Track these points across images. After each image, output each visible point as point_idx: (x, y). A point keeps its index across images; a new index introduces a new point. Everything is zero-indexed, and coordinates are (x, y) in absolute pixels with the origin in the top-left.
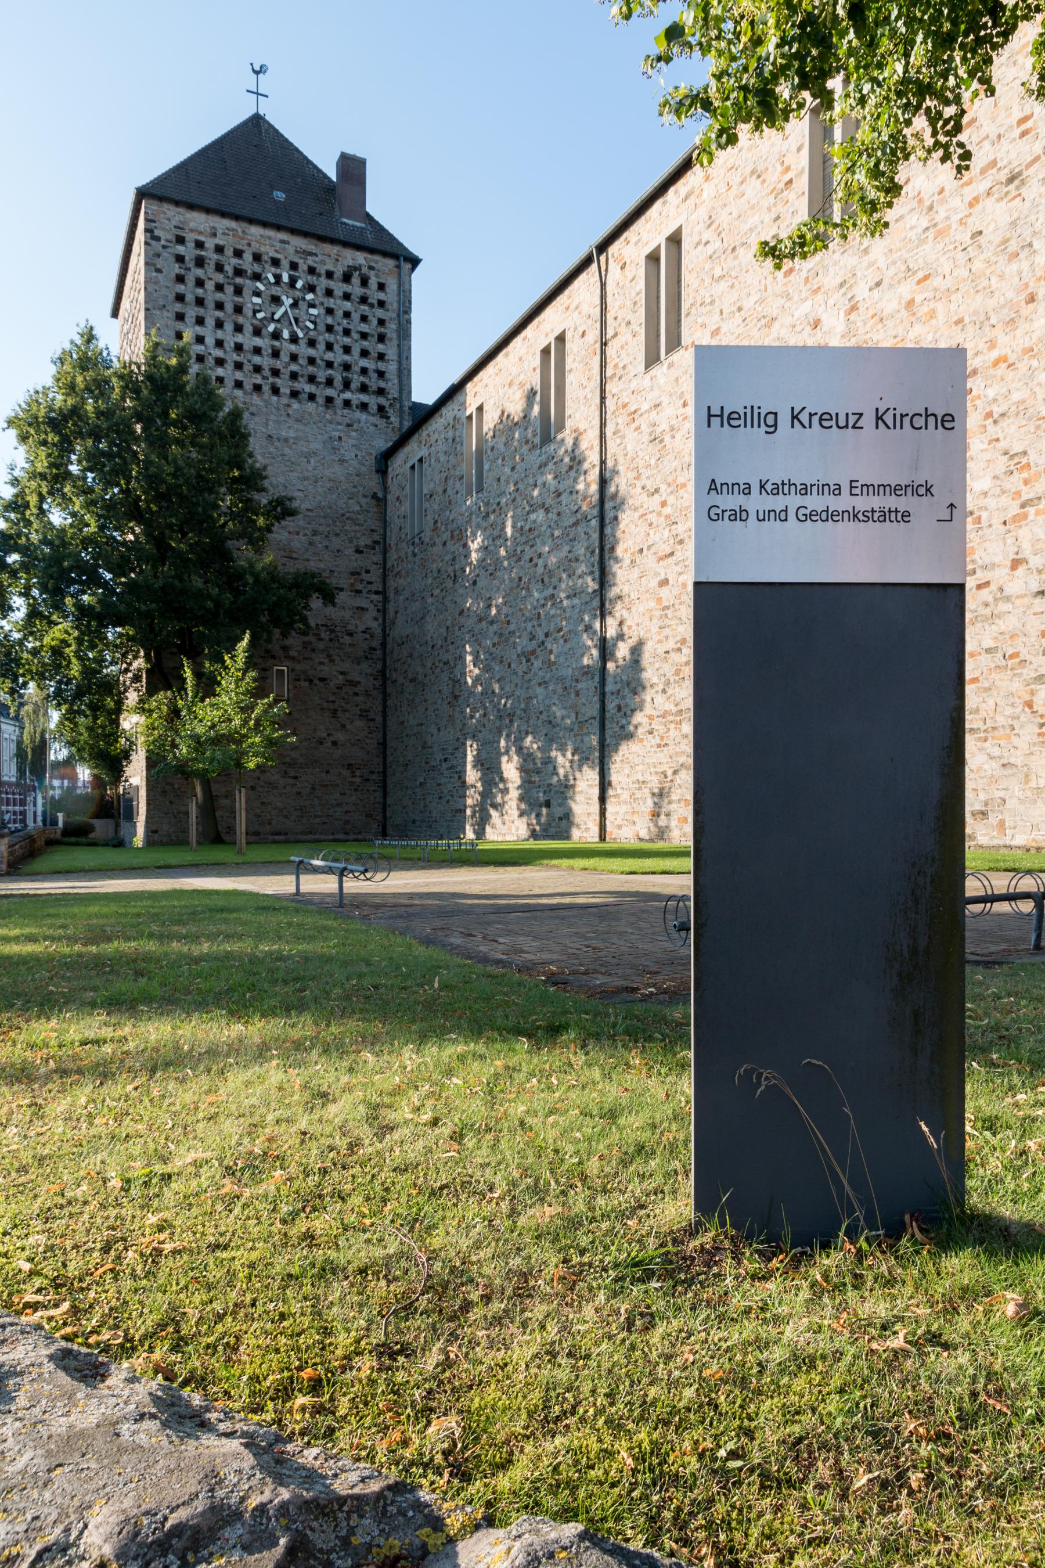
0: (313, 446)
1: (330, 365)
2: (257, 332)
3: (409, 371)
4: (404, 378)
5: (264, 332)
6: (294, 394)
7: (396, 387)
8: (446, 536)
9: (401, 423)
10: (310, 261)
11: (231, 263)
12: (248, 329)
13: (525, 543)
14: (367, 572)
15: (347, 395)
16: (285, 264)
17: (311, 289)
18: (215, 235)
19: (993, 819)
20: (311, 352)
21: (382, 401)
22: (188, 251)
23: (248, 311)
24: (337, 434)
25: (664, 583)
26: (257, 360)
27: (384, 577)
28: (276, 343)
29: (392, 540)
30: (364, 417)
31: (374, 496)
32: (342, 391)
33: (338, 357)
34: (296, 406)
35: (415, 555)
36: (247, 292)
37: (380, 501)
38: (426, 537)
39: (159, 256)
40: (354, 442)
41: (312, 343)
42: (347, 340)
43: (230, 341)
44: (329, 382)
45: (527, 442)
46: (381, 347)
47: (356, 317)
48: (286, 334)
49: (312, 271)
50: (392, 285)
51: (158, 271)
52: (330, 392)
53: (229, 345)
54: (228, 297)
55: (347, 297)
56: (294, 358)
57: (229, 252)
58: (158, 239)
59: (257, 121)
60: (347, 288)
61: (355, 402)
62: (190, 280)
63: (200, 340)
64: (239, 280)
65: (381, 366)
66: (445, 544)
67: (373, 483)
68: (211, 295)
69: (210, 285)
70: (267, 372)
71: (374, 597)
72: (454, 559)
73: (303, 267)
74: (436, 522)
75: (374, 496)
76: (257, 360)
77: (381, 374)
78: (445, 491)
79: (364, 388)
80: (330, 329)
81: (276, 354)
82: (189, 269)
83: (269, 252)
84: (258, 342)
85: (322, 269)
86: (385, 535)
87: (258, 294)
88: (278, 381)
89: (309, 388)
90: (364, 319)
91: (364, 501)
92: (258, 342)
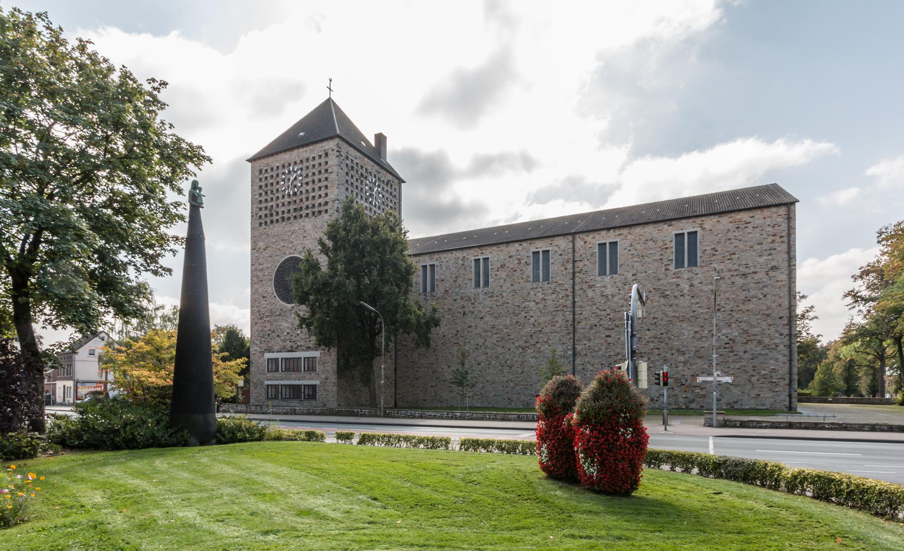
25: (609, 336)
54: (358, 184)
59: (329, 102)
68: (355, 184)
87: (366, 185)
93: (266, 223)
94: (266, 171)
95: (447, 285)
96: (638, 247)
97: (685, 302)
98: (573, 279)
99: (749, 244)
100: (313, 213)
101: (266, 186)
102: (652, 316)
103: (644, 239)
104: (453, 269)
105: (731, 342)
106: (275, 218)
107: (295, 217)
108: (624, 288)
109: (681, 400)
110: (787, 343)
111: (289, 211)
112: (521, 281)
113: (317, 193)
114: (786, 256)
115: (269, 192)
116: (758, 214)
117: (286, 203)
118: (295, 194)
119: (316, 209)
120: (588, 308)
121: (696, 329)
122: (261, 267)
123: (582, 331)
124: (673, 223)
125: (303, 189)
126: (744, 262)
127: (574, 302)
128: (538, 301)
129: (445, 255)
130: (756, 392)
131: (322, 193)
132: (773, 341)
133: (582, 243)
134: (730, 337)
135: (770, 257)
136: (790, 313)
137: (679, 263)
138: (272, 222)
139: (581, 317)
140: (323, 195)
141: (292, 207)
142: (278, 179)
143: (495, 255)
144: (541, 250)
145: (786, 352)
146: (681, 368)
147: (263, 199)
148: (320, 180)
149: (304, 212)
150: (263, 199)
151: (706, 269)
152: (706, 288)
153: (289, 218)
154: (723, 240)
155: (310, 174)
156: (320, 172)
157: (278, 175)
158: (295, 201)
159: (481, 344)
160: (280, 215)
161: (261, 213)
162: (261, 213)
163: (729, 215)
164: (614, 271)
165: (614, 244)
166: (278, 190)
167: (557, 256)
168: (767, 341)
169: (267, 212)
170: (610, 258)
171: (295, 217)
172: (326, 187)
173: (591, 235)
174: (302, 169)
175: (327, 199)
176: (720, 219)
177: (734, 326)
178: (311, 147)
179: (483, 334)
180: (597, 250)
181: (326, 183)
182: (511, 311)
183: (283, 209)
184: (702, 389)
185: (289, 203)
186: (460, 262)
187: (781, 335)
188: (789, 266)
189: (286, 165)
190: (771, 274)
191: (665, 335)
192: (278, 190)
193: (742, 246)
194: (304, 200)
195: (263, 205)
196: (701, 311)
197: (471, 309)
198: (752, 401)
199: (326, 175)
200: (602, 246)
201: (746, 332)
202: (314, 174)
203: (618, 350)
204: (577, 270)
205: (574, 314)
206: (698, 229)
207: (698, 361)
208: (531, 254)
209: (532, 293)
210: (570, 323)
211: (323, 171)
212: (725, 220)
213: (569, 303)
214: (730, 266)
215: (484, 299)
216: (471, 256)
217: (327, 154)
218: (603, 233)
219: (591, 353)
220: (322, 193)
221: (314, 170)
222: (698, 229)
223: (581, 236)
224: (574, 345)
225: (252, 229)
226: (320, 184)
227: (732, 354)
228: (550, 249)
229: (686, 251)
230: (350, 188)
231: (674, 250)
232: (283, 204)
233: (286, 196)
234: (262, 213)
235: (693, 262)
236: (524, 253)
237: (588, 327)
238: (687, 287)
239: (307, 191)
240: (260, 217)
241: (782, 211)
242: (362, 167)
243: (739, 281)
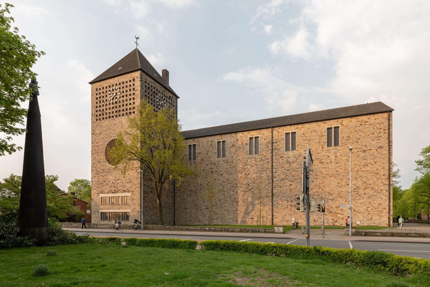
12: (156, 106)
36: (156, 98)
50: (175, 101)
54: (152, 97)
68: (151, 97)
69: (150, 94)
85: (166, 96)
87: (157, 98)
93: (100, 119)
94: (100, 89)
95: (203, 156)
96: (307, 135)
97: (332, 166)
99: (367, 134)
100: (127, 114)
101: (100, 98)
102: (315, 174)
103: (310, 130)
104: (206, 147)
105: (357, 188)
106: (105, 116)
107: (116, 116)
108: (299, 158)
110: (388, 189)
111: (113, 112)
113: (128, 102)
114: (387, 141)
115: (102, 101)
116: (372, 117)
117: (111, 108)
118: (116, 102)
119: (128, 111)
120: (280, 169)
121: (339, 181)
122: (97, 144)
123: (277, 182)
124: (326, 122)
125: (121, 100)
126: (364, 144)
127: (272, 166)
128: (253, 165)
129: (201, 139)
131: (132, 102)
132: (379, 188)
133: (277, 132)
134: (357, 185)
135: (378, 141)
136: (389, 172)
137: (329, 145)
138: (103, 118)
139: (276, 174)
140: (132, 103)
141: (115, 110)
142: (107, 94)
143: (228, 139)
144: (254, 137)
145: (387, 194)
146: (330, 203)
147: (98, 105)
148: (130, 95)
149: (121, 113)
150: (98, 105)
151: (344, 147)
152: (343, 158)
153: (113, 117)
154: (353, 131)
155: (125, 91)
156: (130, 90)
157: (106, 92)
158: (116, 107)
159: (221, 189)
160: (108, 115)
161: (97, 113)
162: (97, 113)
163: (356, 118)
164: (294, 148)
165: (294, 133)
166: (106, 100)
167: (263, 140)
168: (376, 187)
169: (101, 113)
170: (292, 141)
171: (116, 116)
172: (134, 98)
174: (120, 88)
175: (134, 106)
176: (351, 120)
177: (359, 179)
179: (222, 184)
180: (284, 137)
181: (133, 96)
183: (109, 111)
185: (113, 108)
187: (384, 184)
188: (389, 146)
189: (111, 86)
190: (379, 150)
191: (322, 185)
192: (106, 100)
193: (363, 135)
194: (121, 106)
195: (98, 109)
196: (341, 171)
197: (216, 170)
199: (134, 92)
200: (287, 134)
201: (365, 183)
202: (127, 91)
203: (296, 193)
204: (274, 148)
205: (272, 173)
206: (340, 125)
208: (249, 139)
209: (249, 161)
210: (270, 177)
211: (132, 89)
212: (354, 120)
213: (270, 166)
214: (357, 146)
216: (216, 139)
217: (134, 80)
218: (288, 127)
219: (282, 194)
220: (132, 102)
221: (127, 89)
222: (340, 125)
223: (276, 128)
224: (272, 190)
225: (92, 123)
226: (130, 97)
227: (358, 195)
228: (259, 136)
229: (333, 138)
231: (326, 137)
232: (110, 108)
233: (111, 104)
234: (98, 113)
235: (336, 144)
236: (244, 138)
237: (280, 180)
238: (334, 158)
239: (123, 101)
240: (97, 115)
241: (386, 115)
242: (154, 88)
243: (362, 154)
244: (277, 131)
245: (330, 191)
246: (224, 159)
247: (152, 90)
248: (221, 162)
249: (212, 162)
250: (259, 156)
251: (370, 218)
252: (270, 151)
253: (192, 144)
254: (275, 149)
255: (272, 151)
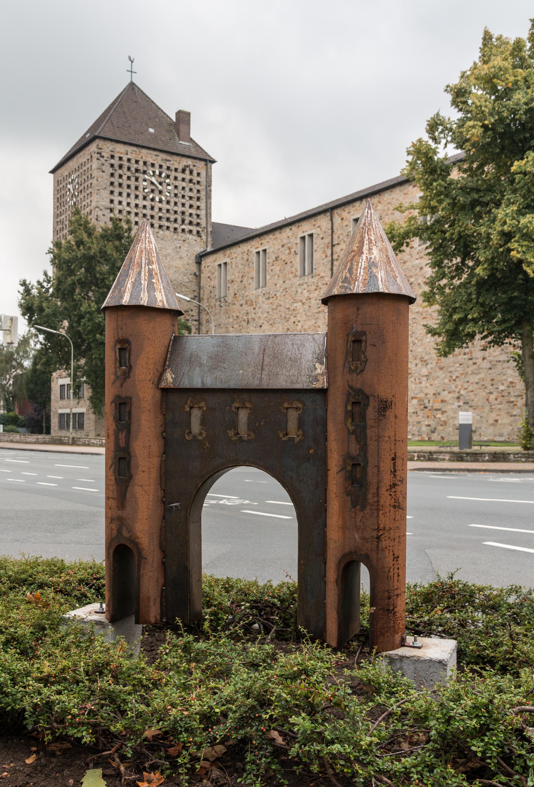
0: (170, 251)
1: (176, 212)
2: (145, 198)
3: (211, 214)
4: (208, 217)
5: (148, 198)
6: (160, 227)
7: (205, 222)
8: (243, 302)
9: (207, 239)
10: (168, 164)
11: (134, 167)
12: (141, 197)
13: (291, 315)
14: (192, 310)
15: (183, 227)
16: (157, 166)
17: (168, 177)
18: (127, 154)
19: (477, 433)
20: (168, 207)
21: (199, 229)
22: (116, 162)
23: (141, 189)
24: (178, 245)
26: (144, 211)
27: (199, 313)
28: (153, 203)
29: (205, 295)
30: (190, 237)
31: (195, 274)
32: (181, 225)
33: (179, 209)
34: (161, 232)
35: (221, 307)
36: (140, 180)
37: (198, 276)
38: (230, 299)
39: (103, 164)
40: (187, 249)
41: (168, 202)
42: (183, 201)
43: (133, 202)
44: (176, 221)
45: (292, 273)
46: (198, 203)
47: (187, 189)
48: (157, 199)
49: (168, 168)
51: (103, 172)
52: (176, 225)
53: (133, 205)
54: (133, 183)
55: (183, 180)
56: (160, 209)
57: (133, 161)
58: (103, 157)
60: (183, 176)
61: (187, 230)
62: (117, 175)
63: (120, 203)
64: (137, 175)
65: (198, 212)
66: (241, 305)
67: (194, 268)
68: (125, 182)
69: (125, 177)
70: (149, 217)
71: (195, 323)
72: (247, 313)
73: (165, 167)
74: (235, 294)
75: (195, 274)
76: (144, 211)
77: (198, 216)
78: (242, 281)
79: (191, 223)
80: (176, 195)
81: (152, 208)
82: (116, 170)
83: (150, 160)
84: (145, 203)
85: (173, 168)
86: (199, 293)
87: (145, 180)
88: (154, 222)
89: (167, 224)
90: (191, 190)
91: (190, 277)
92: (145, 203)
95: (236, 287)
98: (332, 270)
104: (240, 266)
109: (424, 429)
112: (291, 276)
130: (493, 416)
133: (340, 221)
146: (424, 384)
173: (347, 209)
178: (83, 152)
182: (283, 315)
184: (443, 412)
186: (245, 257)
197: (253, 316)
198: (491, 430)
204: (335, 257)
207: (440, 373)
208: (299, 241)
209: (299, 291)
215: (263, 302)
223: (339, 211)
227: (471, 362)
228: (313, 231)
230: (117, 190)
244: (339, 215)
245: (424, 354)
246: (265, 290)
247: (129, 169)
248: (261, 299)
249: (248, 298)
250: (313, 280)
251: (491, 421)
252: (329, 266)
253: (222, 262)
254: (337, 260)
255: (332, 264)
